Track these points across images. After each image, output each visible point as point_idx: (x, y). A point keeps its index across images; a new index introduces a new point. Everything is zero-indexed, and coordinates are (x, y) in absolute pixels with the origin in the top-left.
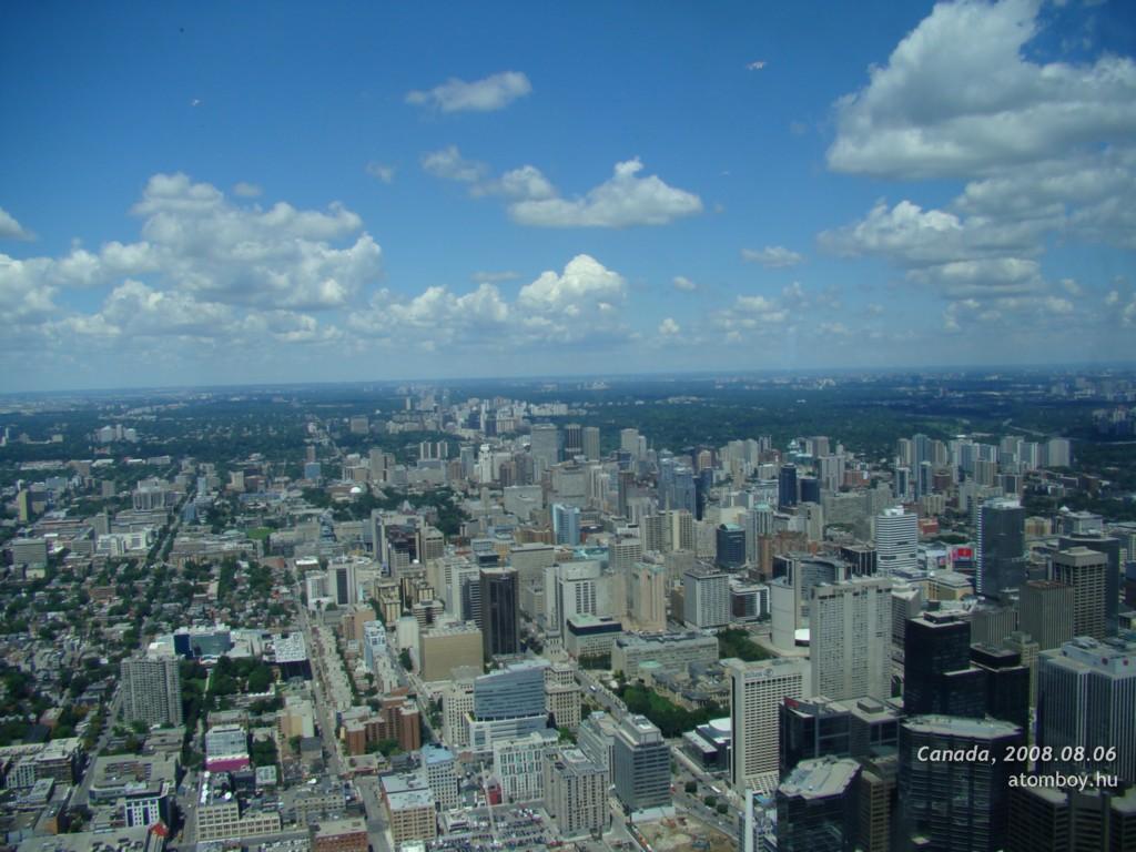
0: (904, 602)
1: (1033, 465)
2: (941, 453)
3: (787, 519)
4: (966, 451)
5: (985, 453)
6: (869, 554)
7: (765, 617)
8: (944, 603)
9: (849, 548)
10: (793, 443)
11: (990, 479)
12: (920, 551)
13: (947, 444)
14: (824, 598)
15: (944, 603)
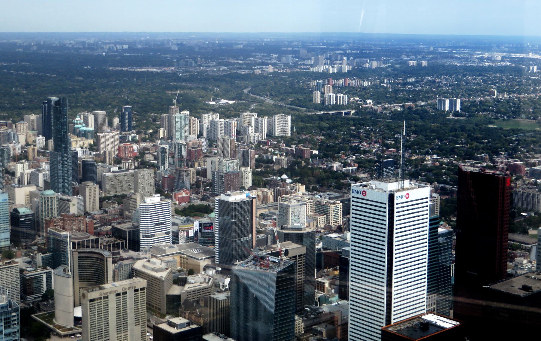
0: (159, 280)
1: (263, 137)
2: (194, 125)
3: (69, 200)
4: (213, 124)
5: (227, 127)
6: (134, 231)
7: (50, 295)
8: (190, 279)
9: (119, 226)
10: (78, 118)
11: (230, 152)
12: (174, 224)
13: (199, 118)
14: (92, 300)
15: (190, 279)
